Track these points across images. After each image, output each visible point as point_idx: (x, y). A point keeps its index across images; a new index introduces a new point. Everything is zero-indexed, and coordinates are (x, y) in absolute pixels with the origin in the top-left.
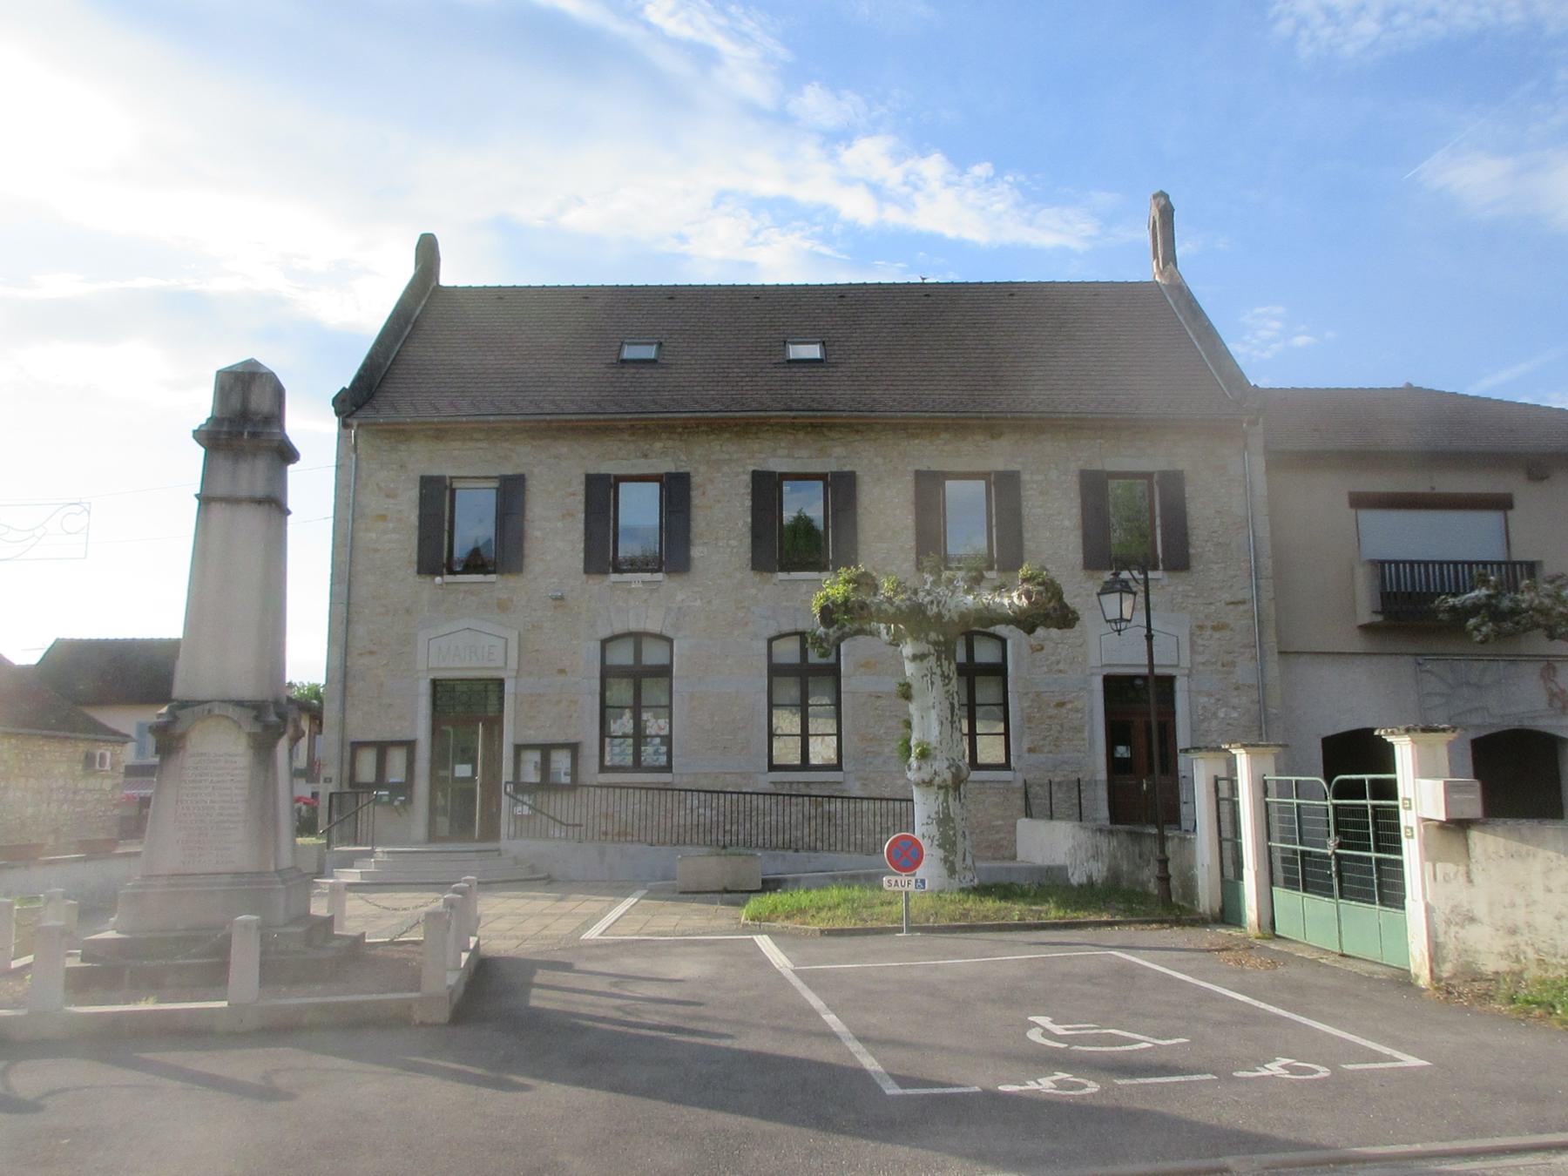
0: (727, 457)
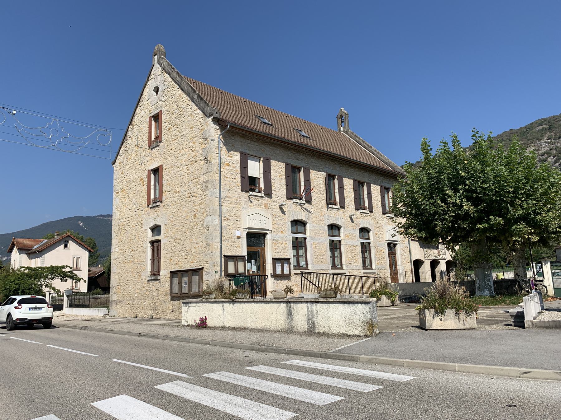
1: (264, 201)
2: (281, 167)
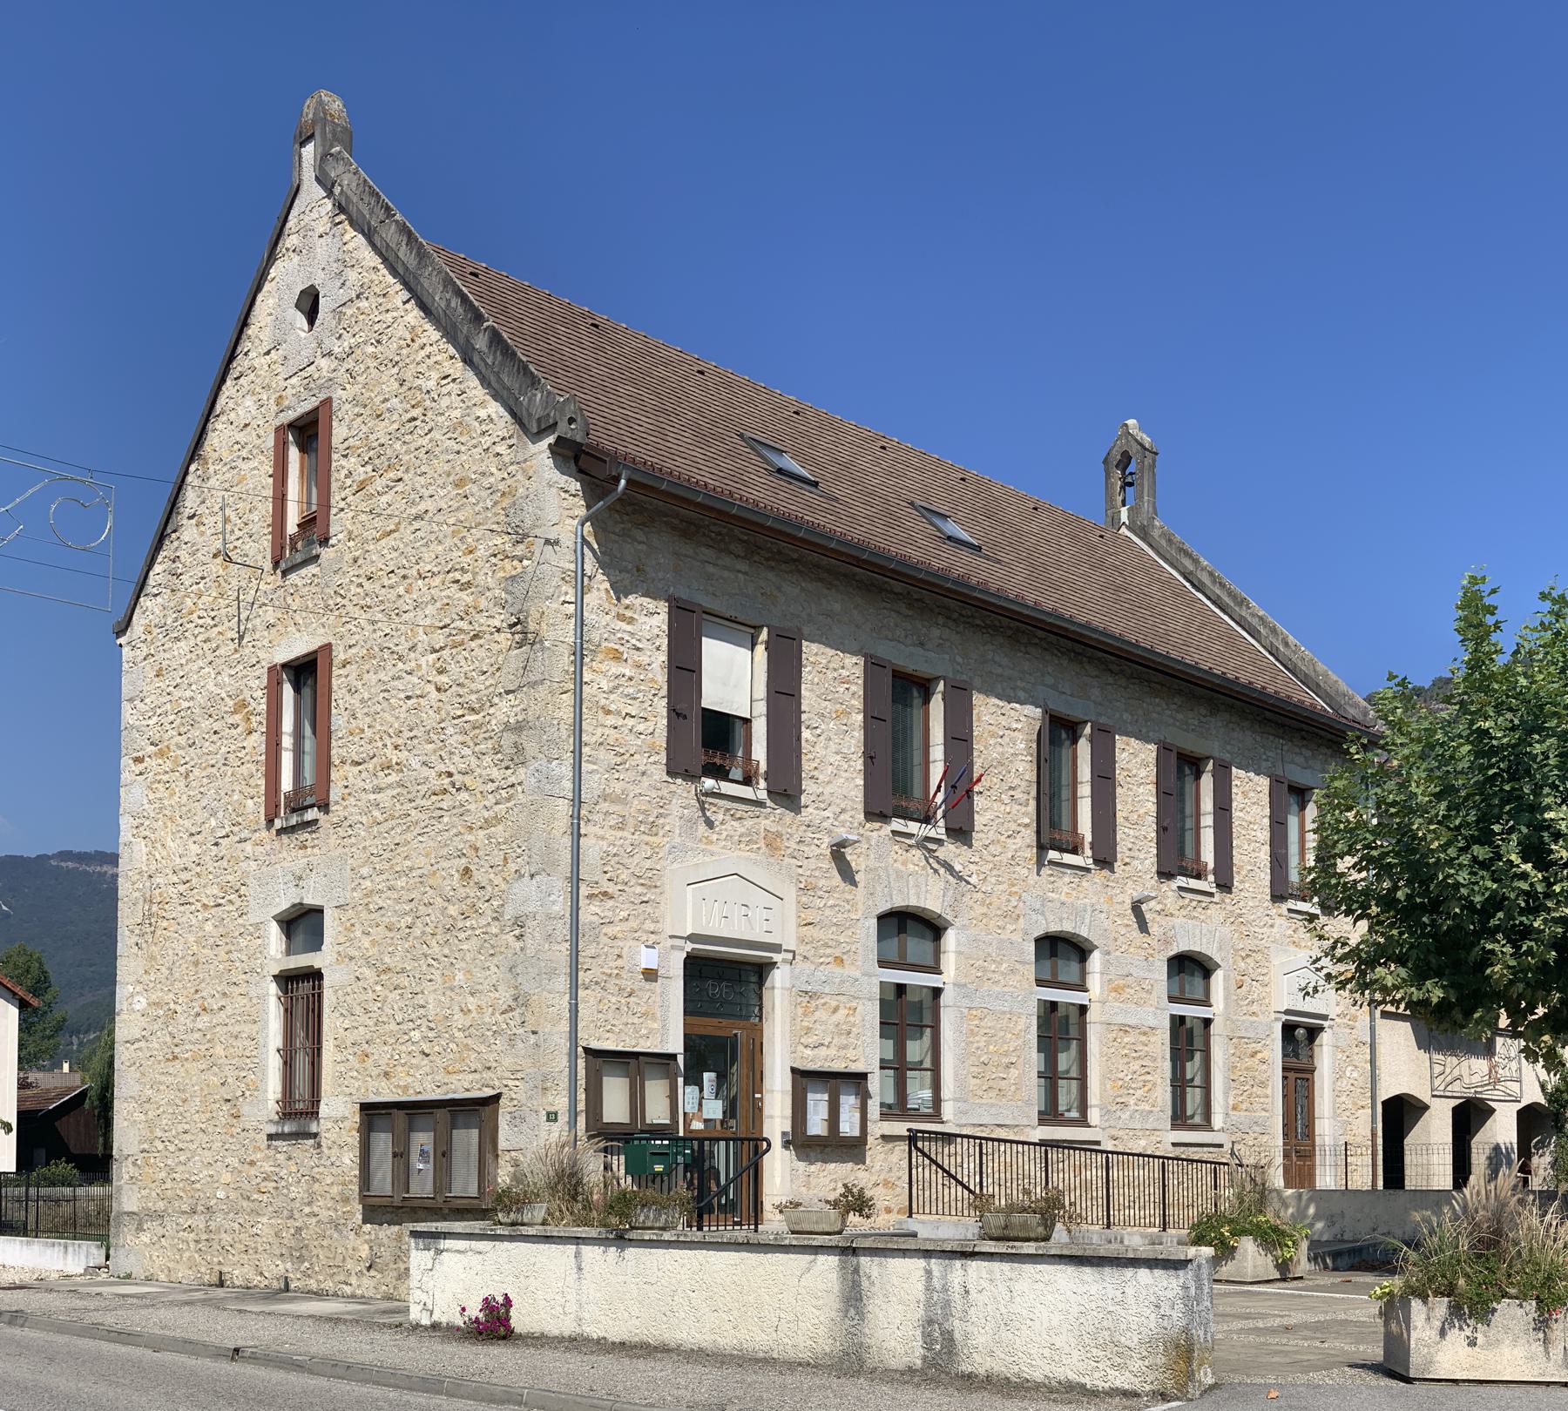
0: (999, 671)
1: (765, 823)
2: (845, 673)
